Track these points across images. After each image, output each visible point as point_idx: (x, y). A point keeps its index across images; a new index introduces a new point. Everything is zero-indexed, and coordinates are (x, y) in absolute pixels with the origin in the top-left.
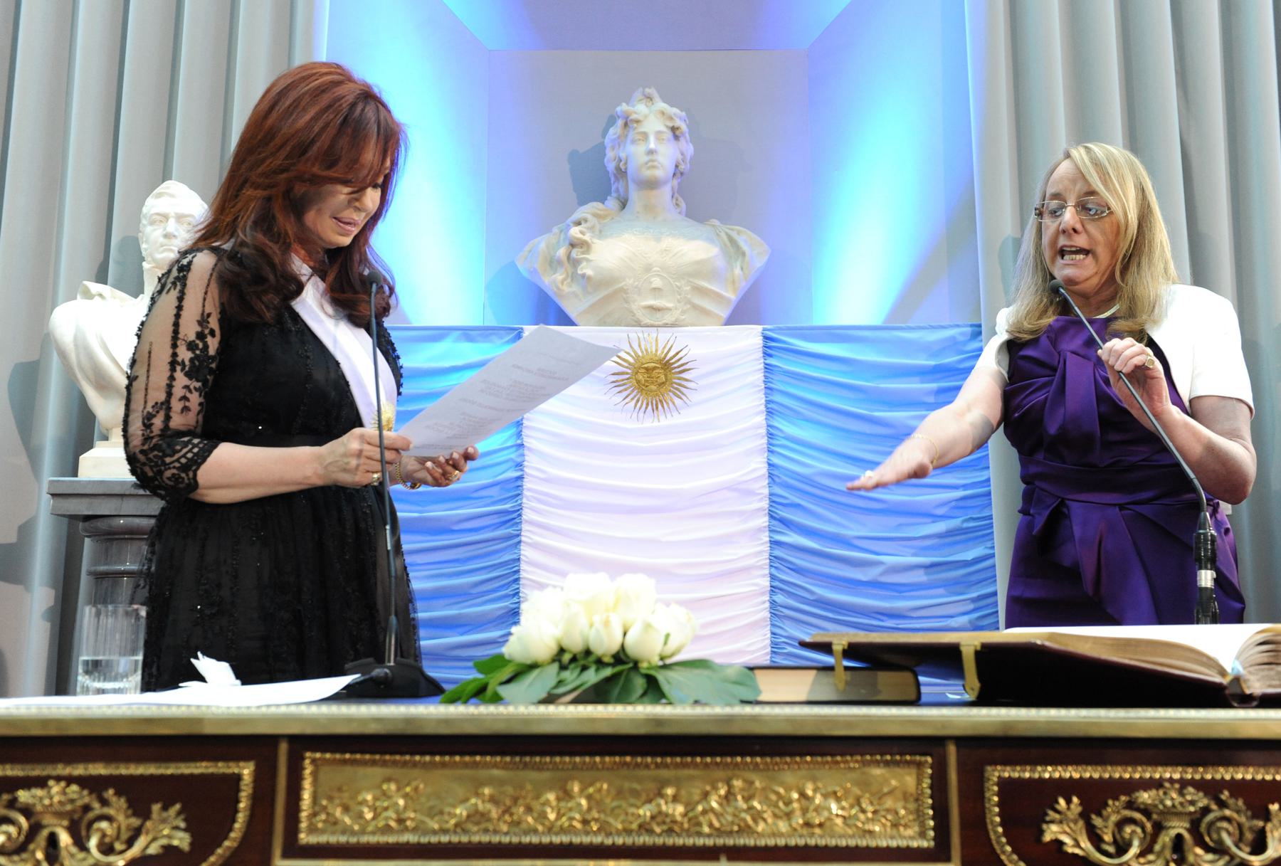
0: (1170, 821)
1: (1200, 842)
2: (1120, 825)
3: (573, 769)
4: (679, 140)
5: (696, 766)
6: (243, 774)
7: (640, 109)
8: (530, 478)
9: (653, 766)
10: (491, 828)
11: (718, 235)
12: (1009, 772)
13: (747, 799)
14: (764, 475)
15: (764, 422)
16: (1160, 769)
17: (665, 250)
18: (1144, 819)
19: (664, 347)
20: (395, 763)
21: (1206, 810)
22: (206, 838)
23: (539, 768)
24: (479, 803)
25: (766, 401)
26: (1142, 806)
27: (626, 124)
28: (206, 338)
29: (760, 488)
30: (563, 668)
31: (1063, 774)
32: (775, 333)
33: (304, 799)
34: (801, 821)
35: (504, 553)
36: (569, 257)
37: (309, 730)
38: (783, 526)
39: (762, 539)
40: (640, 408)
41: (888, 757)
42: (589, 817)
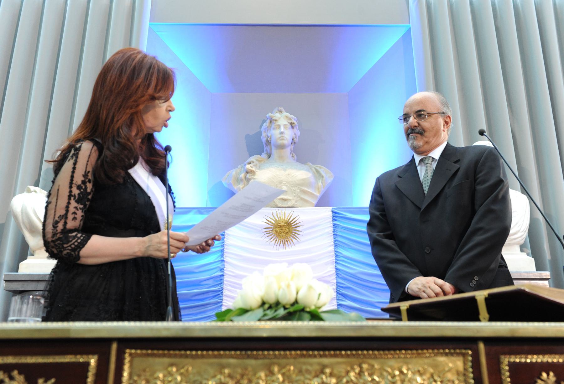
3: (274, 358)
5: (342, 356)
7: (277, 115)
8: (227, 276)
11: (311, 169)
13: (371, 375)
14: (334, 274)
15: (333, 250)
20: (175, 356)
23: (256, 358)
24: (222, 378)
25: (334, 240)
27: (271, 122)
32: (337, 210)
33: (124, 376)
36: (245, 178)
38: (342, 297)
39: (333, 303)
40: (277, 244)
41: (447, 351)
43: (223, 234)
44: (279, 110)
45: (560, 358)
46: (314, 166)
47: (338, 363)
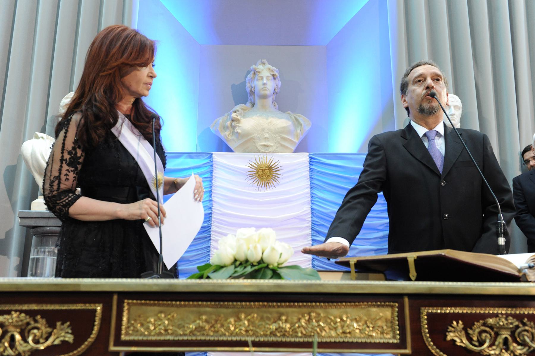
0: (502, 332)
1: (515, 341)
2: (480, 333)
3: (241, 308)
4: (275, 80)
5: (295, 307)
6: (97, 310)
7: (260, 67)
8: (215, 214)
9: (276, 307)
10: (205, 333)
11: (291, 117)
12: (431, 310)
13: (317, 321)
14: (309, 213)
16: (497, 309)
17: (270, 123)
18: (491, 331)
19: (270, 161)
20: (164, 305)
21: (517, 327)
22: (79, 339)
23: (227, 307)
24: (201, 322)
26: (490, 325)
27: (254, 73)
29: (307, 218)
30: (236, 267)
34: (341, 331)
35: (204, 244)
36: (231, 125)
37: (127, 289)
41: (379, 303)
42: (248, 329)
45: (468, 310)
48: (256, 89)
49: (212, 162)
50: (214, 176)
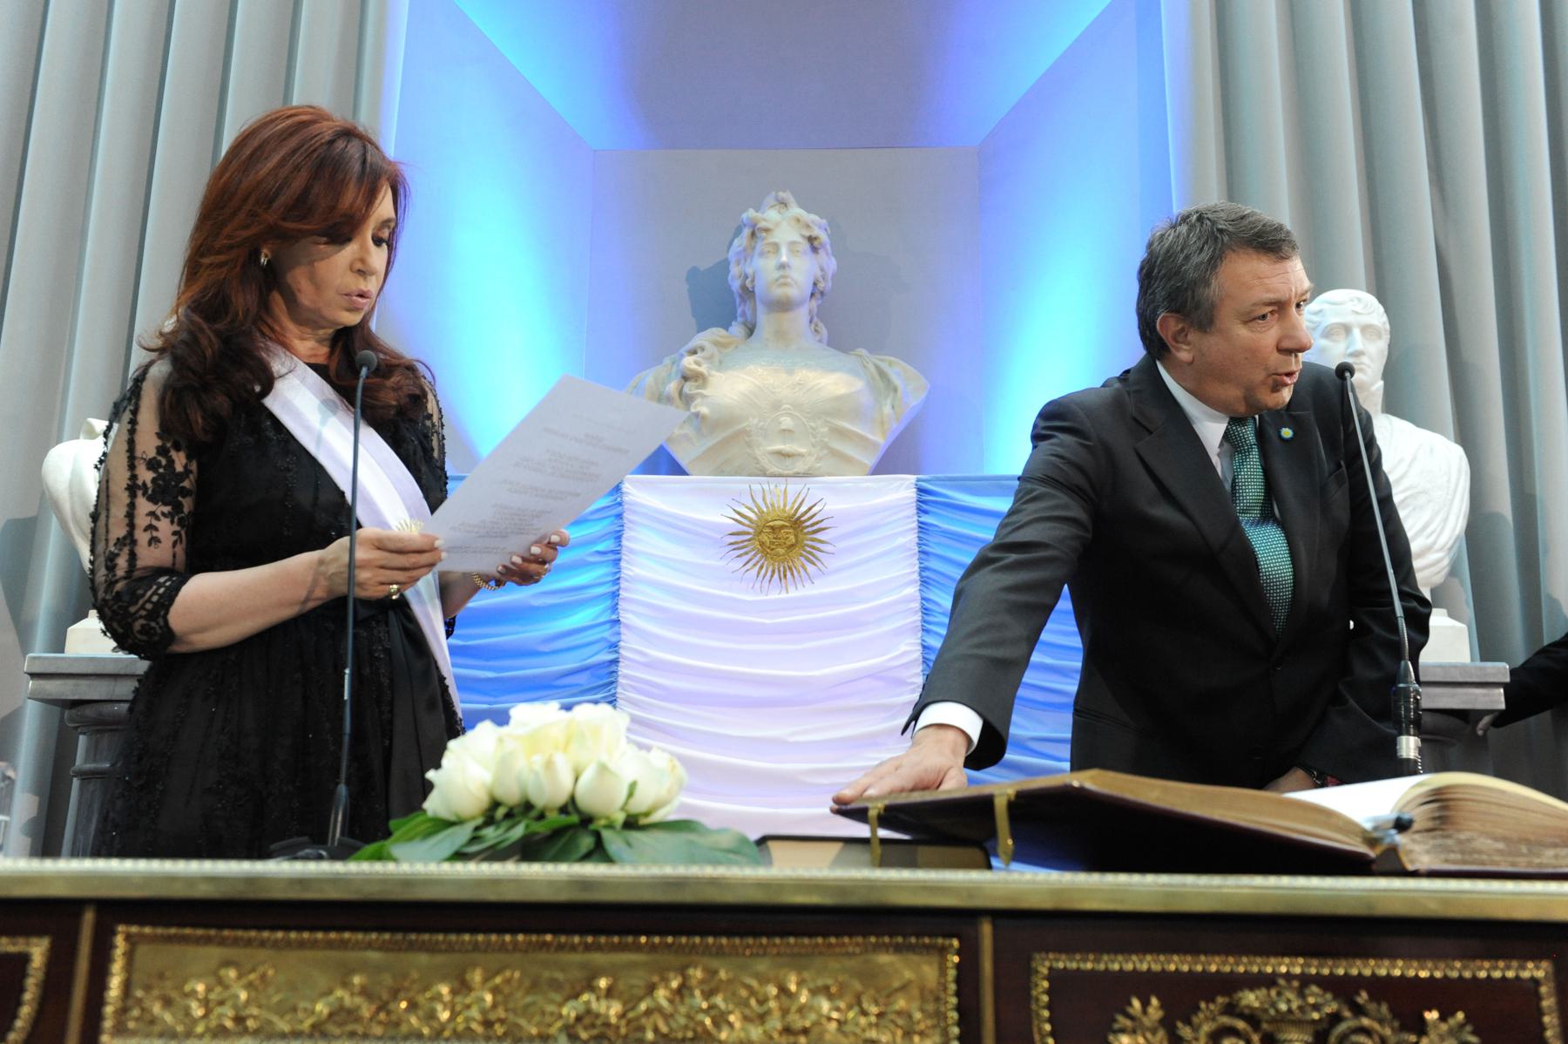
5: (638, 948)
7: (771, 216)
9: (581, 948)
11: (865, 366)
12: (1064, 961)
13: (708, 995)
14: (917, 660)
15: (918, 594)
16: (1273, 960)
17: (799, 384)
20: (236, 942)
21: (1336, 1018)
23: (431, 949)
25: (920, 568)
26: (1247, 1011)
27: (753, 234)
28: (169, 452)
31: (1138, 966)
32: (935, 485)
34: (779, 1026)
36: (681, 393)
40: (764, 577)
41: (900, 940)
42: (492, 1016)
43: (618, 548)
44: (780, 199)
46: (875, 359)
47: (632, 966)
48: (756, 283)
49: (620, 504)
50: (626, 547)
